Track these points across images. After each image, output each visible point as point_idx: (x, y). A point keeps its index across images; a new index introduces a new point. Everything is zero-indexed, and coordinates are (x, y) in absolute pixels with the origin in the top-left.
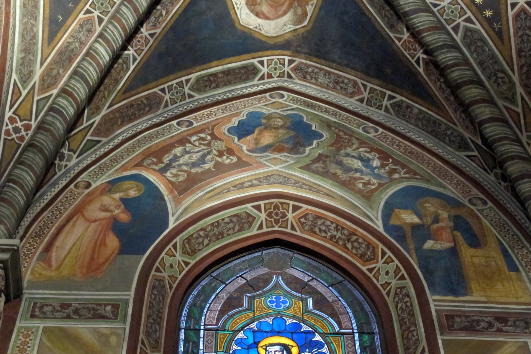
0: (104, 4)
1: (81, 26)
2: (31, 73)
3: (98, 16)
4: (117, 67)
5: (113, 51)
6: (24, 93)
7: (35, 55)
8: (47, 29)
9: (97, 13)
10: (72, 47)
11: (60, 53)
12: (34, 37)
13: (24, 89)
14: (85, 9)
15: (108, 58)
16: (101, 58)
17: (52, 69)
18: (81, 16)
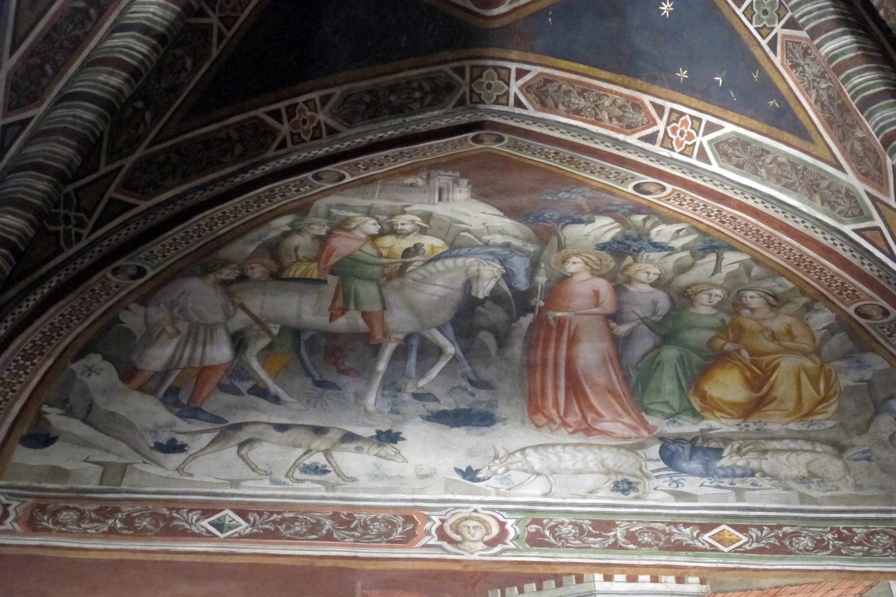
0: (765, 8)
1: (794, 66)
2: (850, 194)
3: (784, 27)
4: (886, 11)
5: (839, 23)
6: (878, 222)
7: (823, 175)
8: (787, 136)
9: (778, 28)
10: (825, 98)
11: (830, 123)
12: (794, 164)
13: (871, 218)
14: (767, 49)
15: (848, 39)
16: (843, 53)
17: (853, 151)
18: (777, 60)
